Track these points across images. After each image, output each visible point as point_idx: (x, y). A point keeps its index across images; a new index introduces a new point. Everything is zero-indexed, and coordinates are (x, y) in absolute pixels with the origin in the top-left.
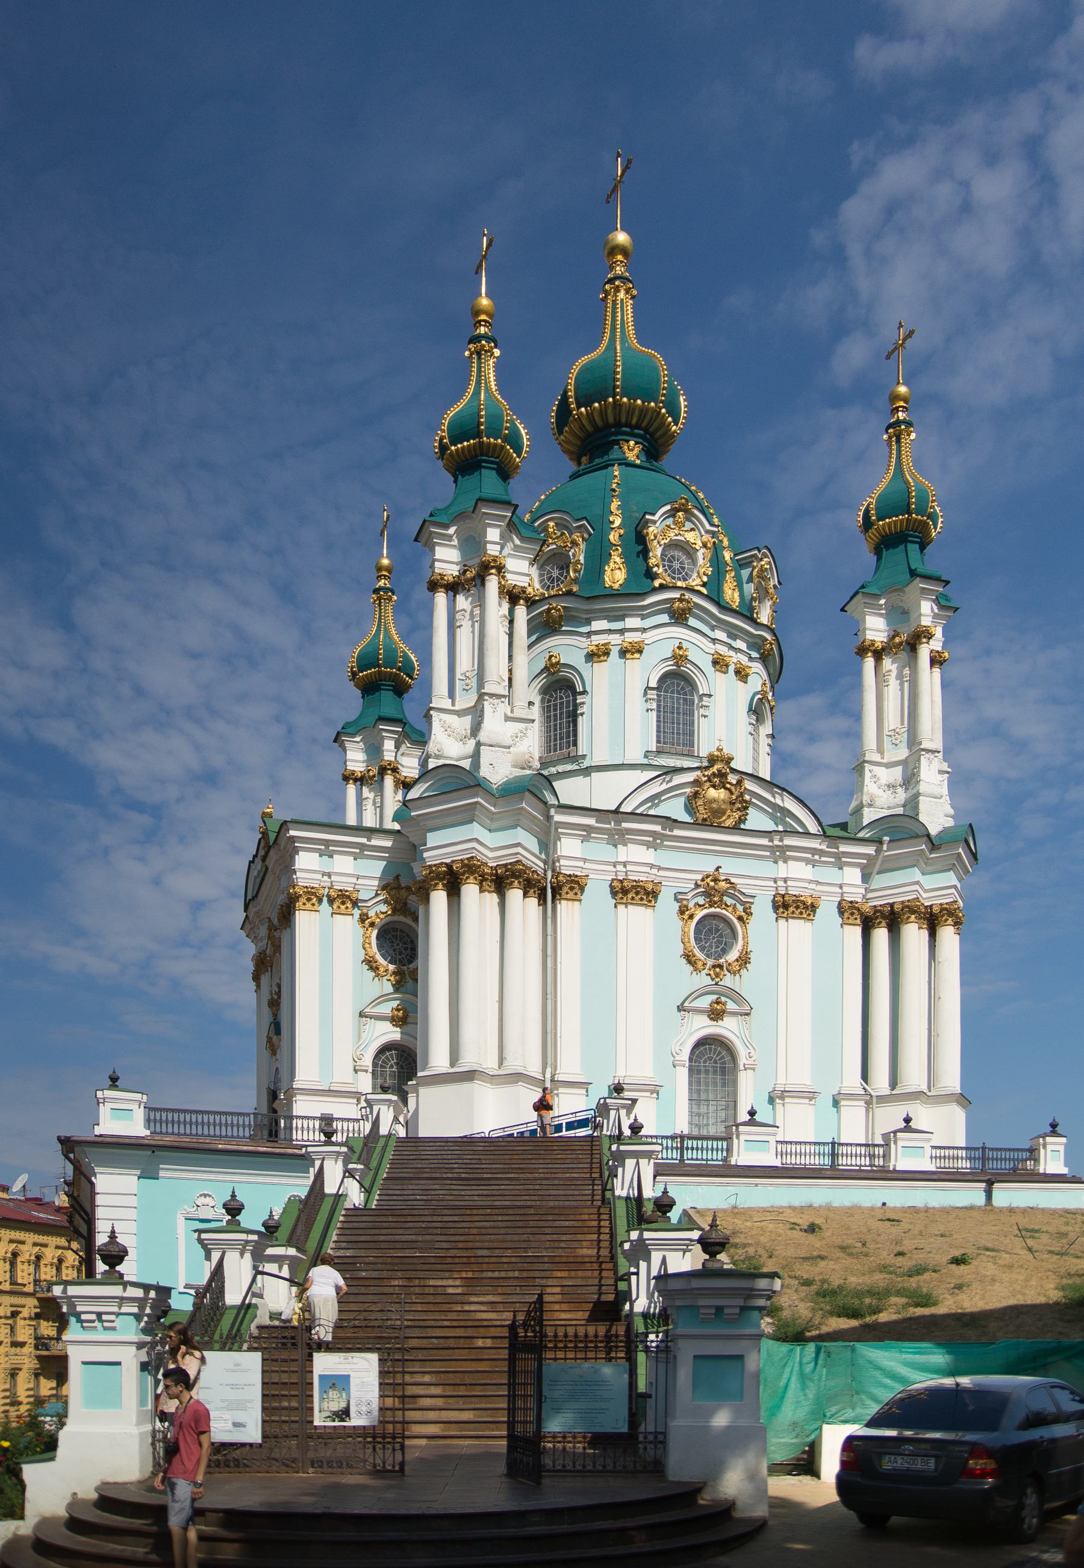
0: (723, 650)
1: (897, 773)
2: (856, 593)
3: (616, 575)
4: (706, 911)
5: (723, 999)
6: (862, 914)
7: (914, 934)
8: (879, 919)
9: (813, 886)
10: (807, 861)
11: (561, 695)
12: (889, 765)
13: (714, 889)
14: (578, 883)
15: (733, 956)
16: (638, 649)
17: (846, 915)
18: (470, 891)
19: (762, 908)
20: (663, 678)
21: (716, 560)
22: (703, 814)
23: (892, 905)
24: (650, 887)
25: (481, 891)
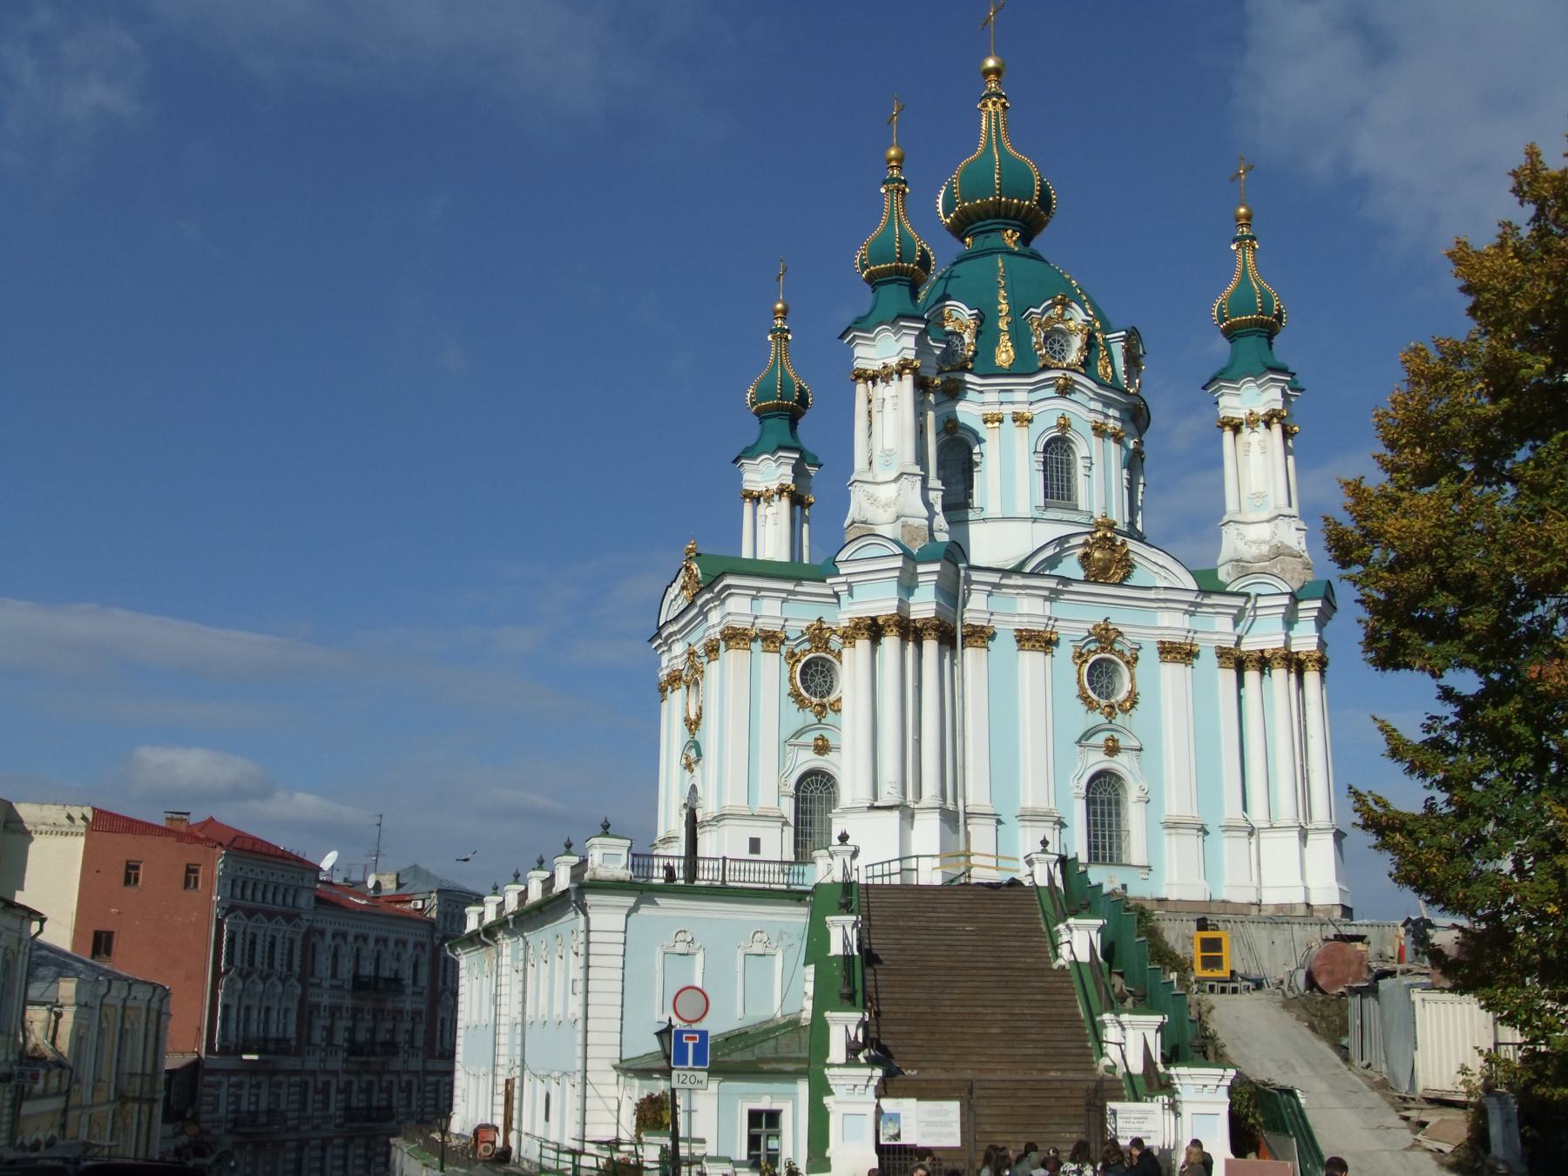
0: (1100, 419)
3: (1004, 355)
5: (1116, 736)
10: (1186, 612)
13: (1105, 636)
15: (1121, 695)
20: (1048, 445)
23: (1262, 651)
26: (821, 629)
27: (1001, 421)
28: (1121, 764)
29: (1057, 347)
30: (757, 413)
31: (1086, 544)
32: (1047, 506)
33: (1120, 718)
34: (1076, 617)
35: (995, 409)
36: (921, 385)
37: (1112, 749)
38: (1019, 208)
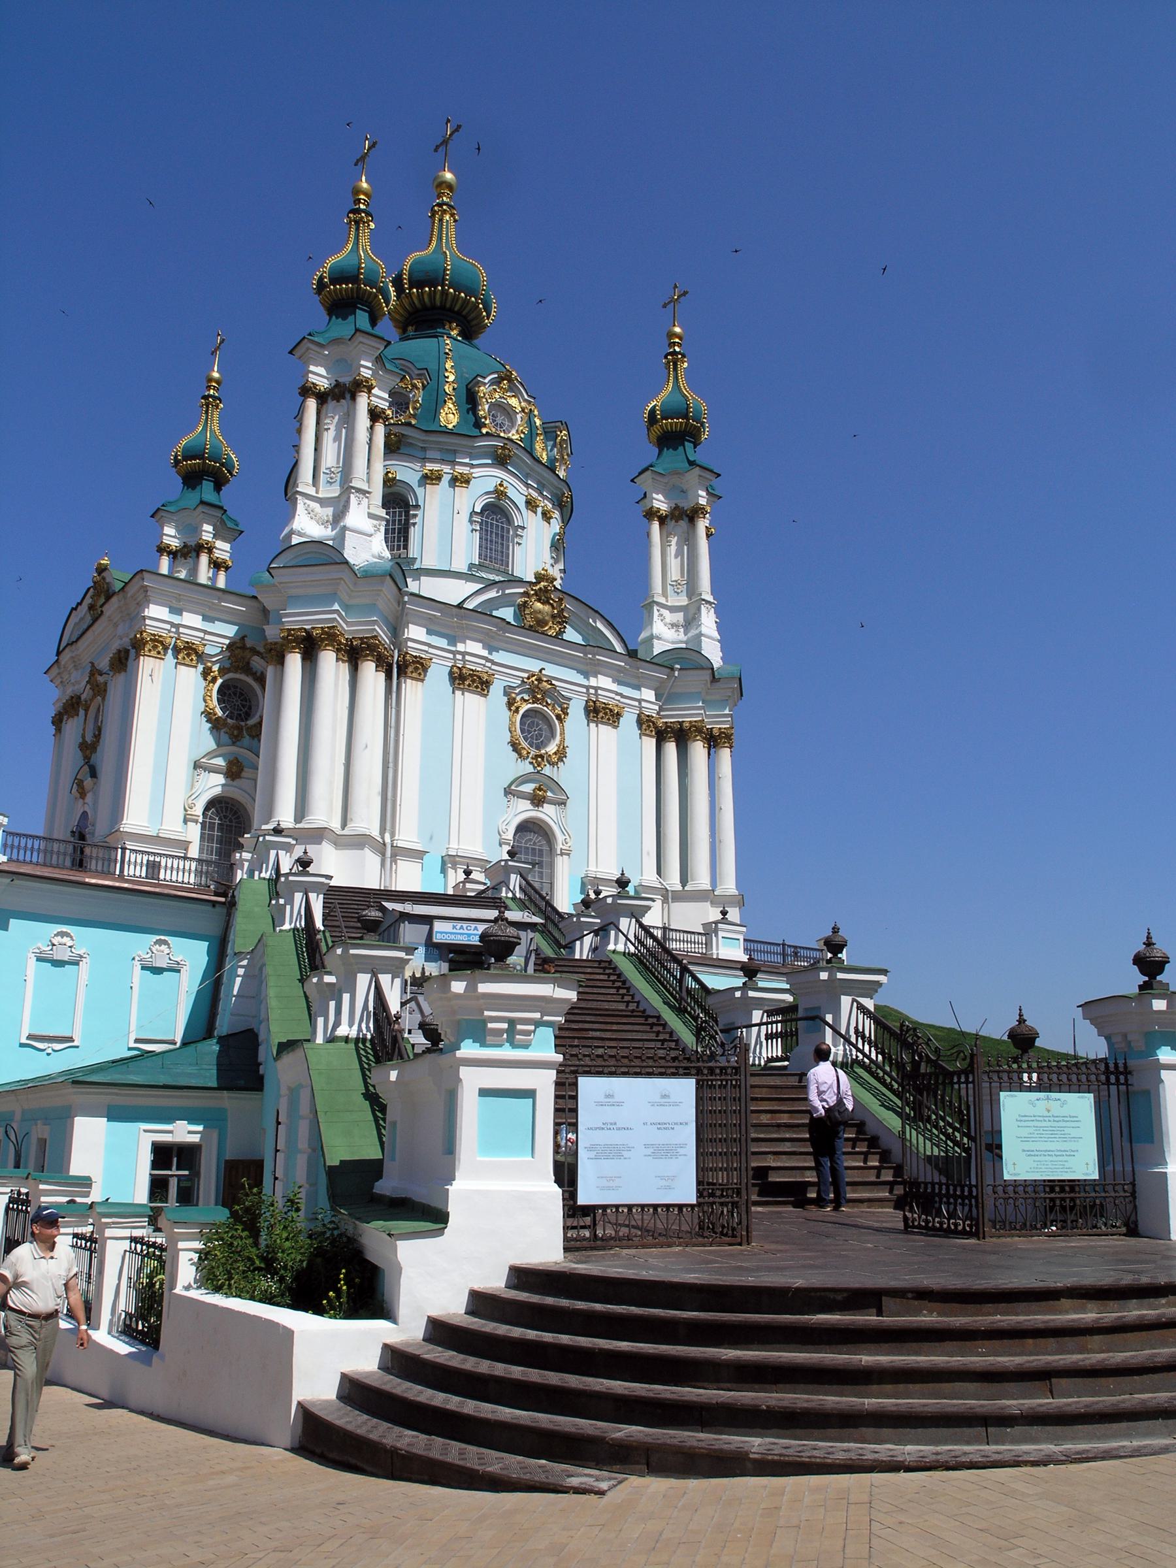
0: (535, 494)
1: (679, 617)
2: (646, 469)
4: (530, 706)
6: (656, 727)
7: (698, 749)
8: (671, 735)
9: (618, 698)
11: (399, 506)
12: (673, 609)
13: (538, 688)
14: (422, 664)
15: (552, 748)
16: (465, 481)
17: (644, 727)
18: (328, 659)
19: (577, 709)
20: (483, 510)
21: (530, 423)
22: (530, 621)
23: (681, 723)
24: (485, 677)
25: (338, 660)
26: (244, 648)
27: (439, 478)
28: (548, 813)
29: (499, 420)
30: (178, 473)
31: (526, 594)
32: (481, 566)
33: (547, 770)
34: (515, 664)
35: (436, 467)
36: (375, 415)
37: (537, 800)
38: (466, 302)
